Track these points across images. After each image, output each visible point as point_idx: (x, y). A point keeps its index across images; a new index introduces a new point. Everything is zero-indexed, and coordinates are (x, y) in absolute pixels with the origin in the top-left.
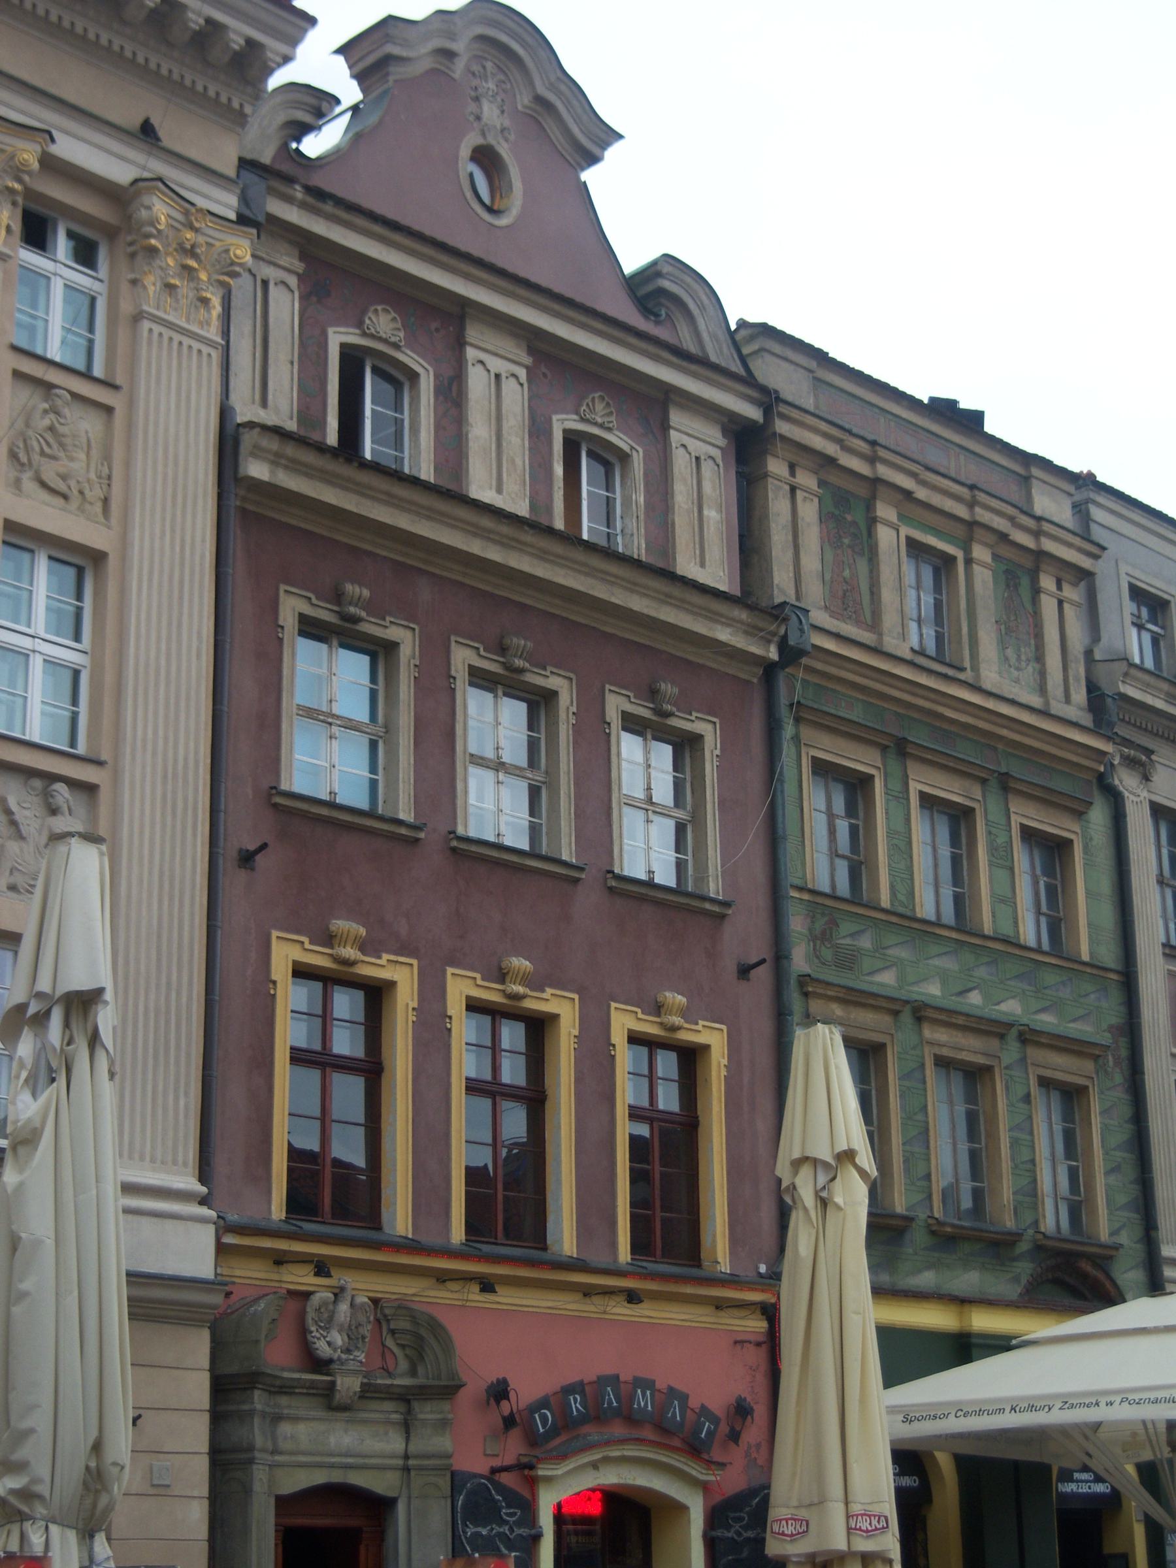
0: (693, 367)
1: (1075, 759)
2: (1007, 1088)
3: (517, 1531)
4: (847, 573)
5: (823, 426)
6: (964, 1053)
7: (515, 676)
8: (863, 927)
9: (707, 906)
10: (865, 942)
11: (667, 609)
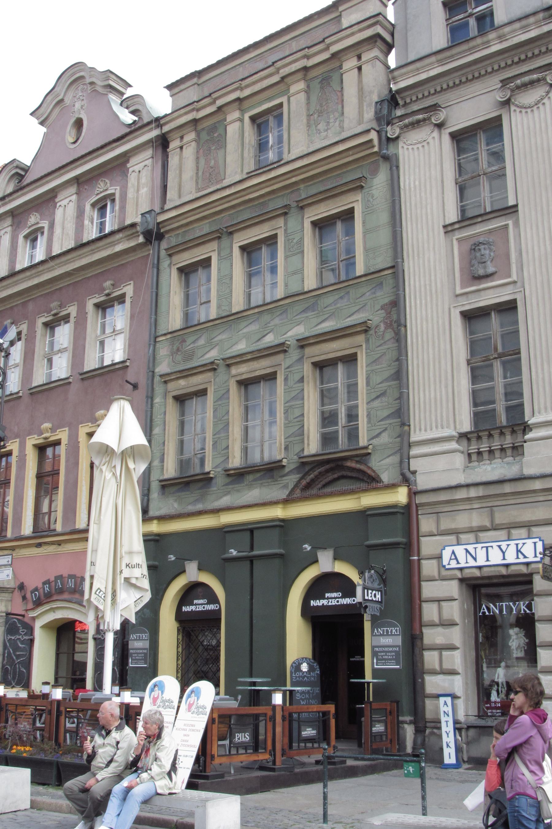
1: (351, 159)
2: (286, 379)
3: (25, 637)
5: (183, 111)
8: (198, 336)
9: (117, 366)
10: (202, 342)
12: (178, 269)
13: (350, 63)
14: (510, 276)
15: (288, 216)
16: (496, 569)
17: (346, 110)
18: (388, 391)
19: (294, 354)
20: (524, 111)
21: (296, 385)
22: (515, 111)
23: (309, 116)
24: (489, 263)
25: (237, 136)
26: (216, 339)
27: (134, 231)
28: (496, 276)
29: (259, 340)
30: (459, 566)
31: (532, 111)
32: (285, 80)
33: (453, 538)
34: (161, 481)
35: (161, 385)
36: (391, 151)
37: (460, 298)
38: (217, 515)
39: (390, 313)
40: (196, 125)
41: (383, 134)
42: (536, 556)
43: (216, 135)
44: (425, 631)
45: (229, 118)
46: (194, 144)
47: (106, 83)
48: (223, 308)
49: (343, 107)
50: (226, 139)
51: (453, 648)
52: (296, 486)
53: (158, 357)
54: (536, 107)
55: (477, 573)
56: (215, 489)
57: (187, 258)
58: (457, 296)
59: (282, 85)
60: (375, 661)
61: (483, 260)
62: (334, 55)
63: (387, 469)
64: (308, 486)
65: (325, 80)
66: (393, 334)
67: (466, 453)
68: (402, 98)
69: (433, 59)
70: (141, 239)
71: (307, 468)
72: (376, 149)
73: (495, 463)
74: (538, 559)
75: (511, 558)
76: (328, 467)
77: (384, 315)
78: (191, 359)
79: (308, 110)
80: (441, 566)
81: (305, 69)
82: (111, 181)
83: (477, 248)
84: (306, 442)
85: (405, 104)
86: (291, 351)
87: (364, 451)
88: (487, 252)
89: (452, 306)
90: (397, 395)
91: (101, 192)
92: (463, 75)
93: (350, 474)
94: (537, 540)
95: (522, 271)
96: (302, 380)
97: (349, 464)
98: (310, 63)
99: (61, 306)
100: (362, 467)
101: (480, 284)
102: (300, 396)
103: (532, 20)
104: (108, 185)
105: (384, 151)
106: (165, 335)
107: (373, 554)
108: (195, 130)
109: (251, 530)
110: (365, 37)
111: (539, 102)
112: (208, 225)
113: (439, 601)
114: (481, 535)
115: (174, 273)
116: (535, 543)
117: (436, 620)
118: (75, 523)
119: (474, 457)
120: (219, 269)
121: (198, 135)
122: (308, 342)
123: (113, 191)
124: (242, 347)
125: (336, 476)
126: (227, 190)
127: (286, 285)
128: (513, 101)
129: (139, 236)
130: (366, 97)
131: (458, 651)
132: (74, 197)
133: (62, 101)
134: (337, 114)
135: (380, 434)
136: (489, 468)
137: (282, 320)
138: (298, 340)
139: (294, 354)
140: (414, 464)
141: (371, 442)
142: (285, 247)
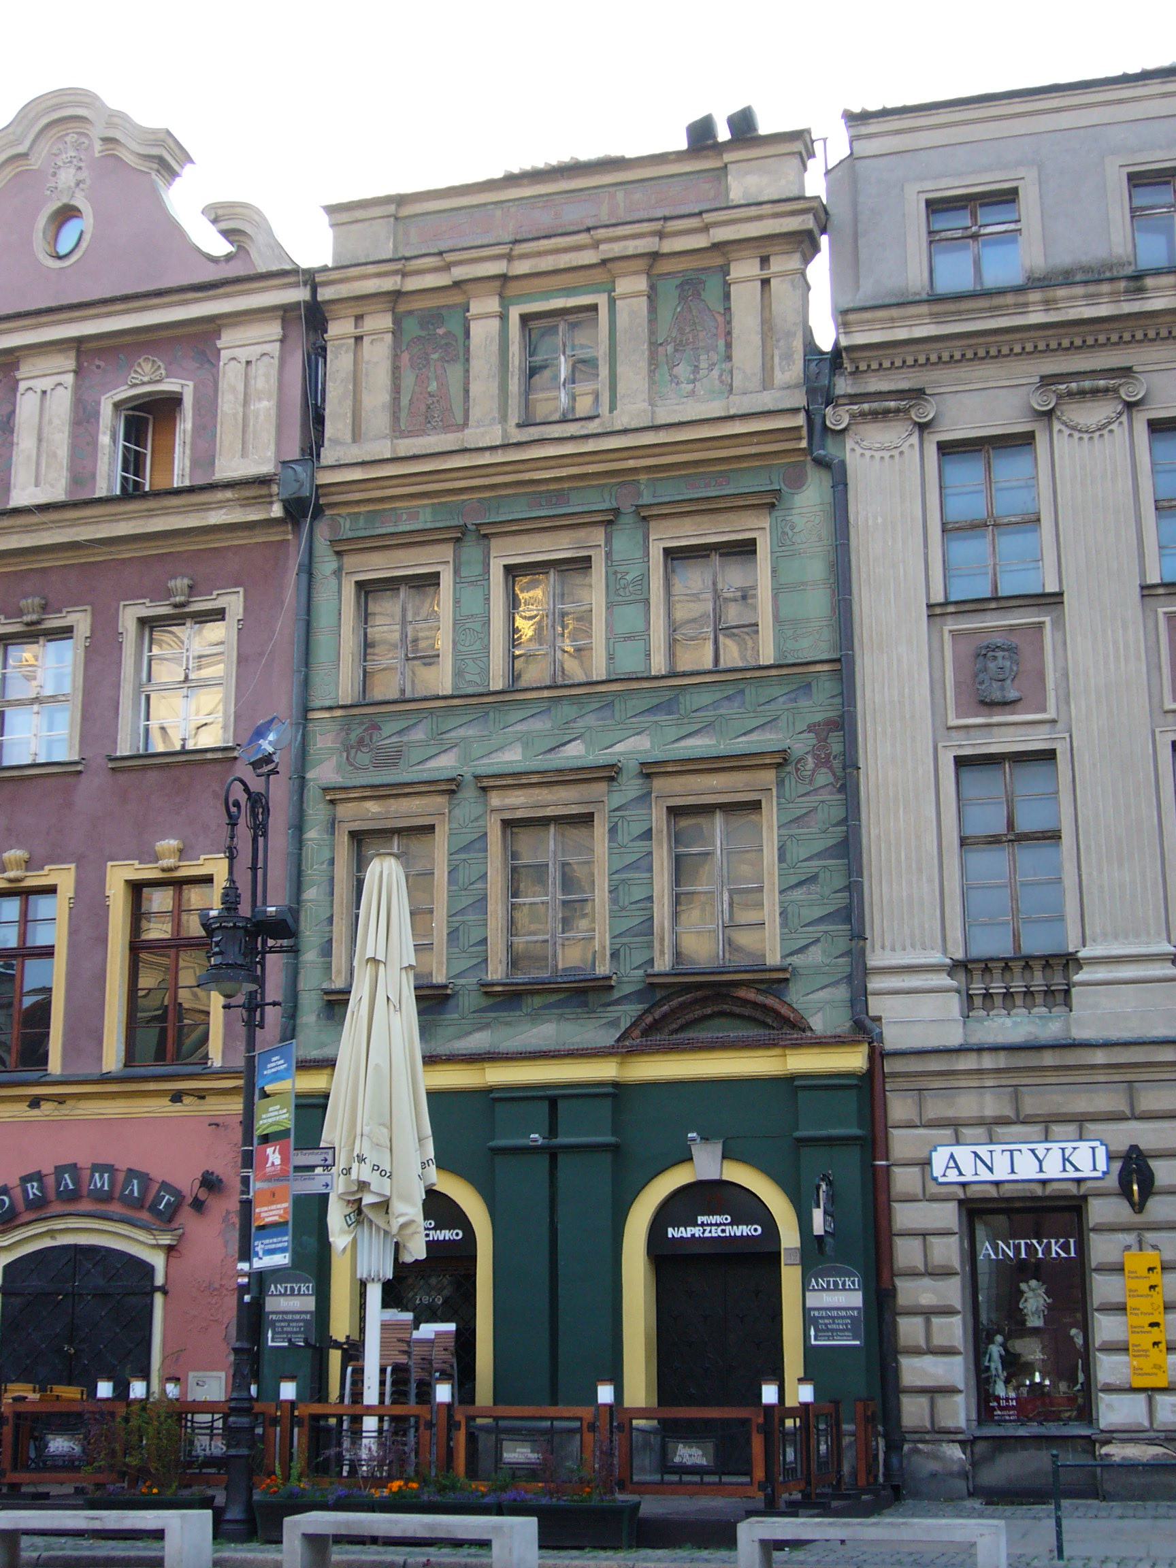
0: (221, 291)
2: (613, 831)
4: (433, 386)
5: (371, 269)
6: (549, 809)
7: (32, 628)
9: (209, 756)
10: (418, 735)
11: (155, 520)
12: (356, 582)
13: (744, 269)
14: (1043, 709)
15: (614, 527)
16: (1027, 1186)
17: (737, 353)
18: (821, 875)
19: (630, 787)
20: (1076, 435)
21: (635, 844)
22: (1060, 431)
23: (654, 345)
24: (1009, 682)
25: (495, 347)
26: (453, 734)
27: (264, 491)
28: (1019, 706)
29: (553, 749)
30: (962, 1179)
31: (1091, 438)
32: (609, 265)
33: (948, 1132)
34: (327, 993)
35: (321, 806)
36: (830, 449)
37: (954, 733)
38: (478, 1066)
39: (825, 740)
40: (395, 302)
41: (818, 420)
42: (1095, 1169)
43: (440, 331)
44: (902, 1284)
45: (476, 307)
46: (389, 338)
47: (155, 151)
48: (468, 677)
49: (729, 346)
50: (467, 349)
51: (948, 1312)
52: (634, 1024)
53: (312, 750)
54: (1098, 433)
55: (993, 1192)
56: (456, 1016)
57: (378, 566)
58: (949, 728)
59: (600, 270)
60: (812, 1333)
61: (1001, 677)
62: (716, 246)
63: (820, 1009)
64: (654, 1027)
65: (690, 286)
66: (831, 779)
67: (964, 993)
68: (852, 360)
69: (924, 309)
70: (277, 511)
71: (659, 994)
72: (804, 444)
73: (1017, 1015)
74: (1099, 1174)
75: (1053, 1169)
76: (699, 994)
77: (815, 742)
78: (395, 764)
79: (652, 332)
80: (928, 1178)
81: (655, 256)
82: (169, 364)
83: (991, 654)
84: (656, 945)
85: (856, 372)
86: (623, 779)
87: (781, 975)
88: (1008, 664)
89: (940, 745)
90: (839, 882)
91: (143, 384)
92: (970, 346)
93: (737, 1010)
94: (1097, 1144)
95: (1068, 703)
96: (648, 835)
97: (742, 993)
98: (668, 246)
99: (45, 608)
100: (770, 1001)
101: (991, 715)
102: (645, 864)
103: (1105, 288)
104: (163, 372)
105: (822, 452)
106: (330, 708)
107: (805, 1152)
108: (393, 310)
109: (551, 1100)
110: (785, 230)
111: (1104, 427)
112: (428, 510)
113: (924, 1235)
114: (1000, 1130)
115: (349, 591)
116: (1093, 1149)
117: (922, 1268)
118: (100, 1058)
119: (978, 1002)
120: (457, 602)
121: (397, 321)
122: (662, 770)
123: (176, 388)
124: (512, 757)
125: (709, 1011)
126: (487, 454)
127: (611, 657)
128: (1059, 414)
129: (271, 503)
130: (778, 341)
131: (959, 1317)
132: (69, 379)
133: (24, 156)
134: (715, 357)
135: (806, 947)
136: (1008, 1022)
137: (603, 719)
138: (641, 764)
139: (630, 787)
140: (876, 1006)
141: (789, 960)
142: (607, 586)
